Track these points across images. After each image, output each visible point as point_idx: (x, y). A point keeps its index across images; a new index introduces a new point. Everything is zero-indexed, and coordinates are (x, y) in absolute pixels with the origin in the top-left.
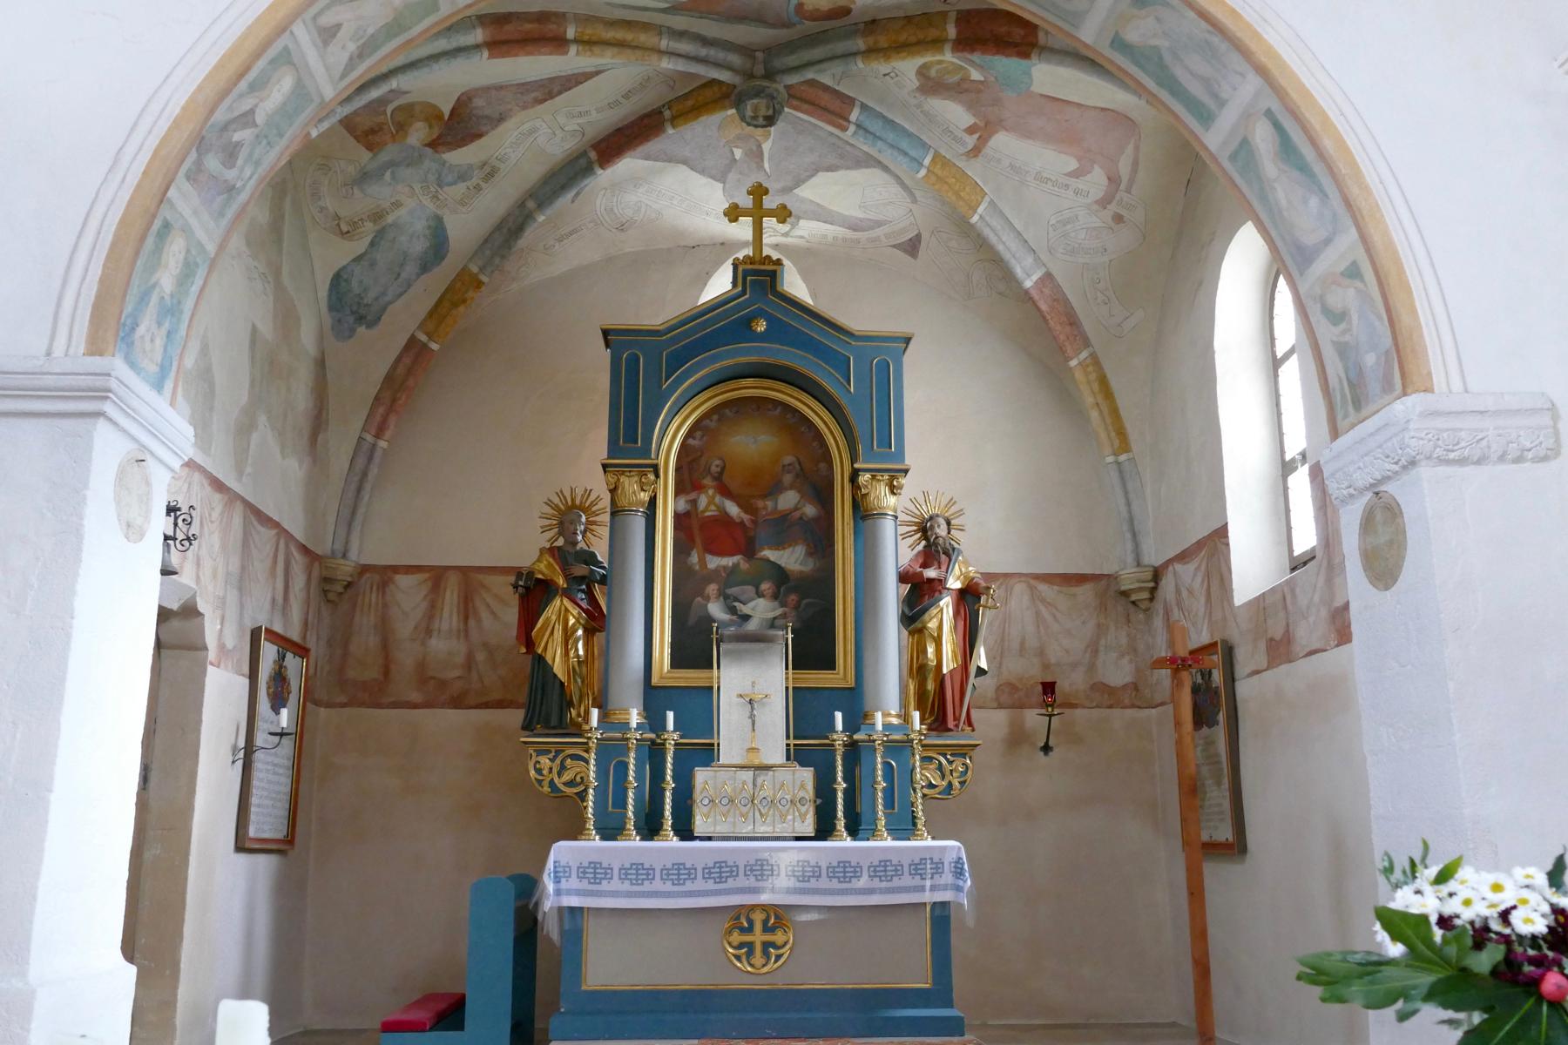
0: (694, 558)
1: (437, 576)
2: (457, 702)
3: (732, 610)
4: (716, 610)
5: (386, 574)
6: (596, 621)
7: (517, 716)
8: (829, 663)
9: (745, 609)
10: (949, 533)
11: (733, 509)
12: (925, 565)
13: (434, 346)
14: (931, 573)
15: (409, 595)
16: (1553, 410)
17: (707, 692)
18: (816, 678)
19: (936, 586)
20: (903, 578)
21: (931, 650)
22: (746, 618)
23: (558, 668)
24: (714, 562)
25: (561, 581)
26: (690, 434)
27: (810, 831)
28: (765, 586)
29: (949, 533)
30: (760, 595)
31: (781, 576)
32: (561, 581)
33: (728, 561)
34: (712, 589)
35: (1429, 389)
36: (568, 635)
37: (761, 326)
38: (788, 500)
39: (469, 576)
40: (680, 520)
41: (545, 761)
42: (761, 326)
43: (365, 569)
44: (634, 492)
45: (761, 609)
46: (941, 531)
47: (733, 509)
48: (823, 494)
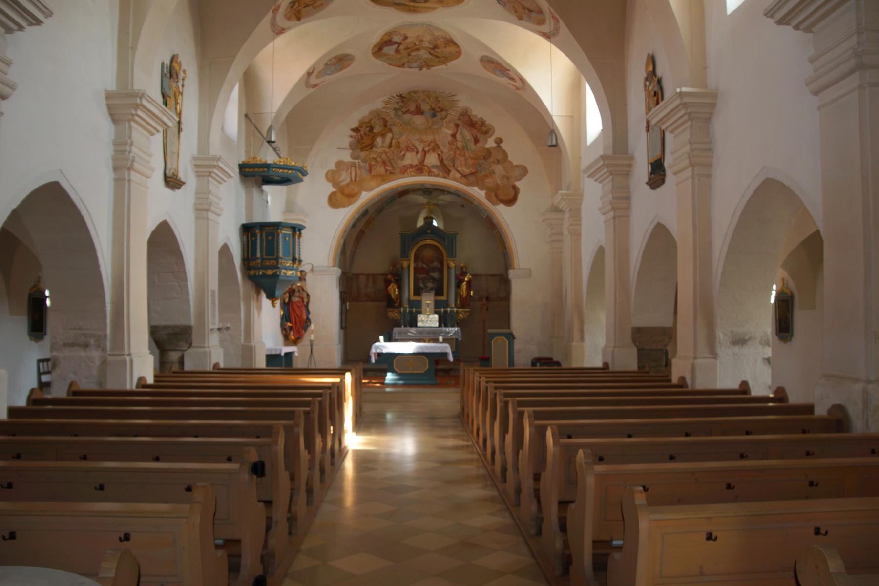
0: (417, 275)
1: (368, 276)
2: (373, 301)
3: (424, 285)
4: (422, 285)
5: (358, 276)
6: (400, 288)
7: (384, 304)
8: (442, 295)
9: (427, 285)
10: (466, 269)
11: (425, 266)
12: (461, 276)
13: (366, 231)
14: (462, 278)
15: (362, 280)
16: (530, 270)
17: (420, 302)
18: (439, 298)
19: (463, 281)
20: (456, 278)
21: (462, 292)
22: (427, 287)
23: (393, 296)
24: (421, 276)
25: (393, 280)
26: (416, 251)
27: (437, 325)
28: (431, 281)
29: (466, 269)
30: (429, 282)
31: (433, 279)
32: (393, 280)
33: (424, 276)
34: (421, 281)
35: (514, 269)
36: (394, 290)
37: (429, 232)
38: (435, 264)
39: (375, 276)
40: (415, 268)
41: (391, 313)
42: (429, 232)
43: (354, 275)
44: (405, 264)
45: (430, 285)
46: (464, 269)
47: (425, 266)
48: (441, 262)
